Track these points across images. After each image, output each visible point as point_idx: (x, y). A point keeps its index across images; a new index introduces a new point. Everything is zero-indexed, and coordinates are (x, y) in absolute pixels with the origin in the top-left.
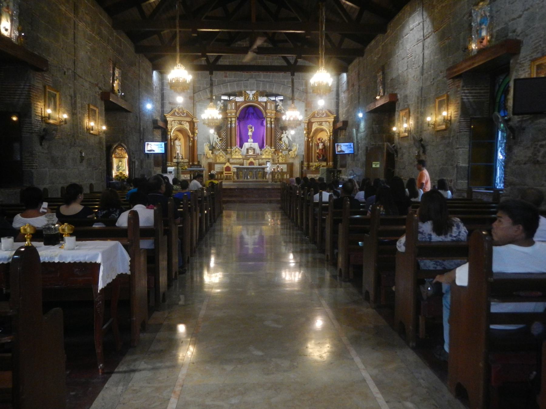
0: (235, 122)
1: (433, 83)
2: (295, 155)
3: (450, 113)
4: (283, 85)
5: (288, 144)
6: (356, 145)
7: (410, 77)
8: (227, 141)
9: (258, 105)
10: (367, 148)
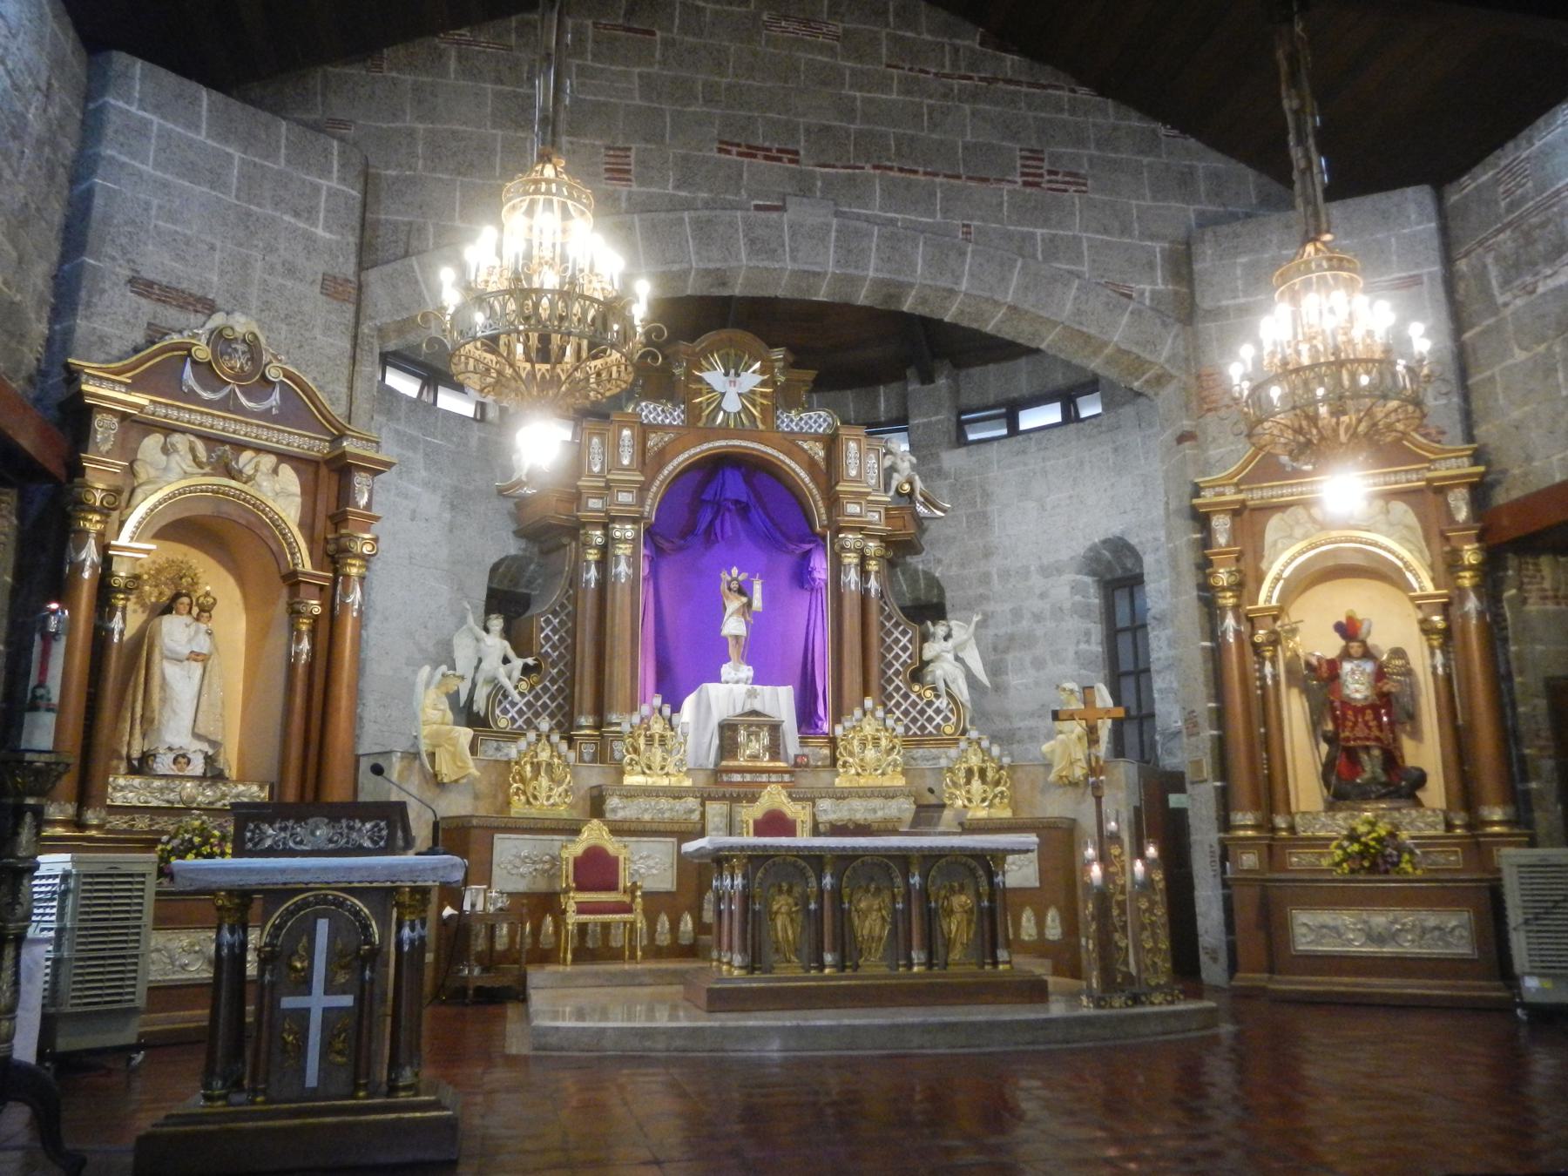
0: (635, 553)
8: (571, 683)
9: (782, 457)
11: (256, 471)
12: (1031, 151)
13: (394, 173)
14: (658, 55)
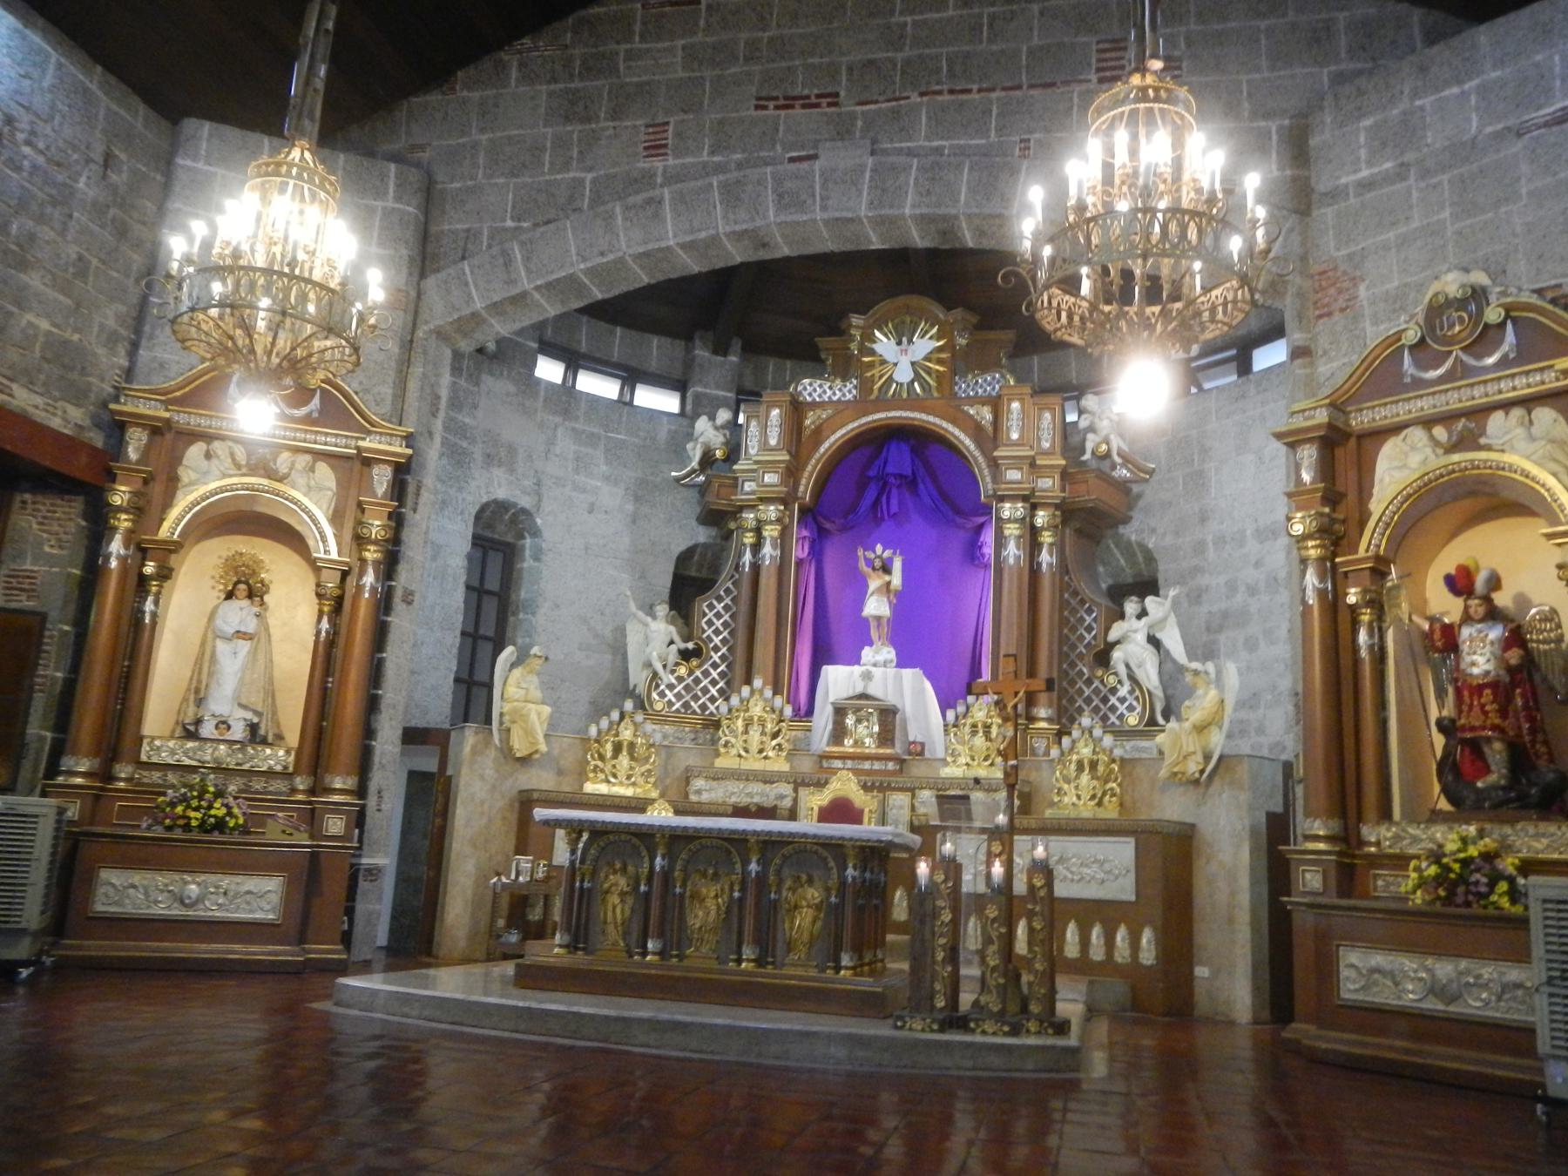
2: (1207, 757)
5: (1159, 693)
9: (945, 424)
11: (291, 469)
12: (1114, 41)
13: (457, 185)
14: (702, 23)
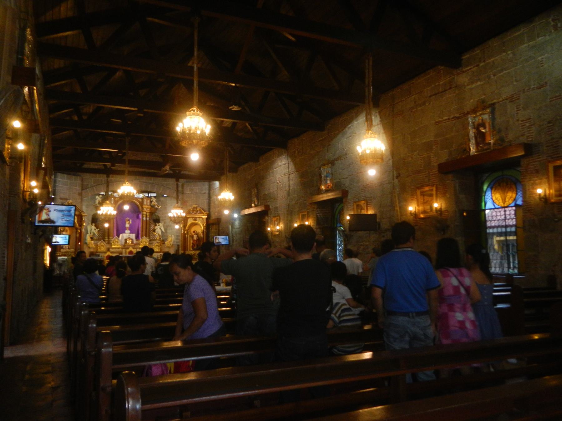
1: (297, 202)
2: (170, 244)
3: (309, 222)
4: (163, 186)
6: (231, 238)
7: (279, 195)
10: (243, 241)
